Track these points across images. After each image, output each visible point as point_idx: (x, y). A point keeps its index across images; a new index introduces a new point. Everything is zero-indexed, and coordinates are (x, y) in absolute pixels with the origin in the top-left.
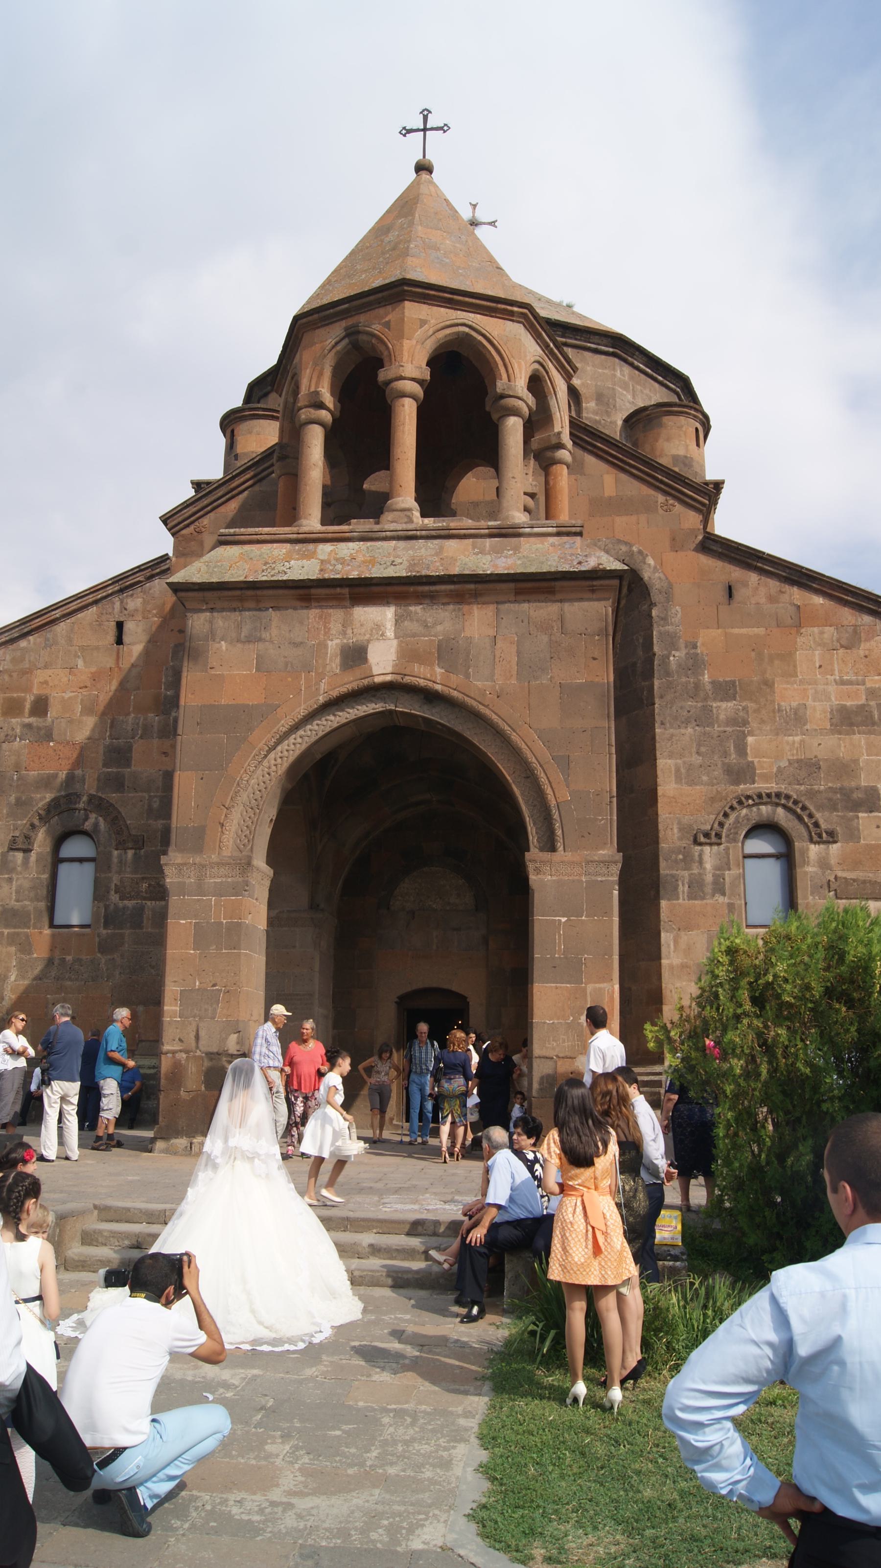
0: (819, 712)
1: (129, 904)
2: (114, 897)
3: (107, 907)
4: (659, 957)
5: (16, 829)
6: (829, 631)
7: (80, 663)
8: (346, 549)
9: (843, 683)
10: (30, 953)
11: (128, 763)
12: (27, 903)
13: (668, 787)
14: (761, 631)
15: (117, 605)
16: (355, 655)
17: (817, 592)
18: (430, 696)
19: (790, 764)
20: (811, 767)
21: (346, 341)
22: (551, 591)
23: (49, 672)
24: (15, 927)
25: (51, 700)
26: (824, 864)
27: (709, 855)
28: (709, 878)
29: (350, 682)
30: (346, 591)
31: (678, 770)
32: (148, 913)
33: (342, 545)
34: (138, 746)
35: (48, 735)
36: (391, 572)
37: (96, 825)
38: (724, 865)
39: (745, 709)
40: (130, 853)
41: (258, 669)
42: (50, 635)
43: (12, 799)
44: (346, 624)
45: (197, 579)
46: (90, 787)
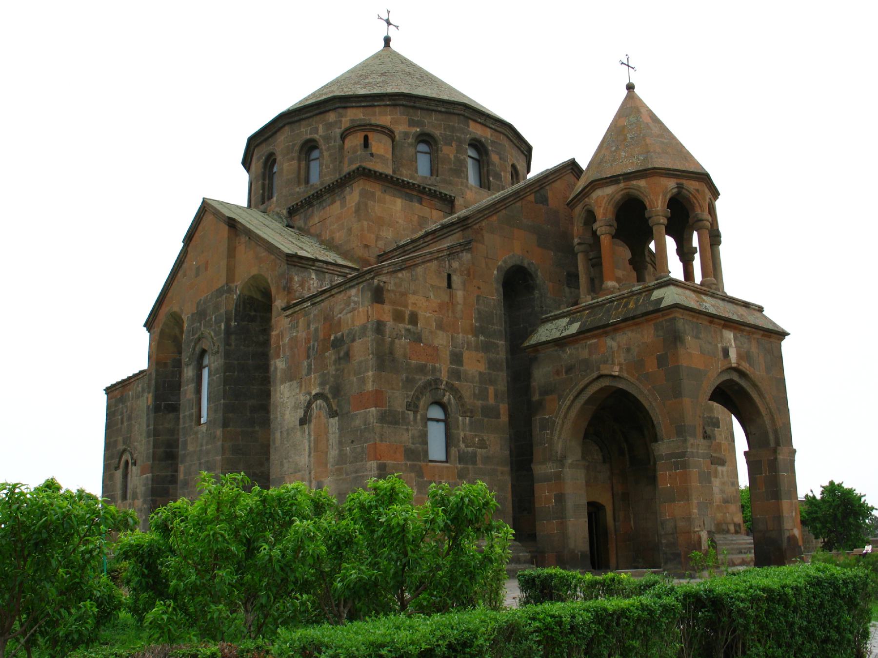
1: (470, 449)
2: (462, 446)
3: (459, 451)
5: (408, 397)
7: (432, 297)
10: (422, 477)
12: (418, 445)
16: (726, 352)
21: (676, 190)
22: (770, 337)
23: (416, 297)
24: (413, 460)
25: (419, 317)
30: (723, 322)
32: (479, 458)
34: (466, 355)
35: (417, 338)
37: (449, 399)
42: (414, 273)
43: (404, 376)
44: (722, 337)
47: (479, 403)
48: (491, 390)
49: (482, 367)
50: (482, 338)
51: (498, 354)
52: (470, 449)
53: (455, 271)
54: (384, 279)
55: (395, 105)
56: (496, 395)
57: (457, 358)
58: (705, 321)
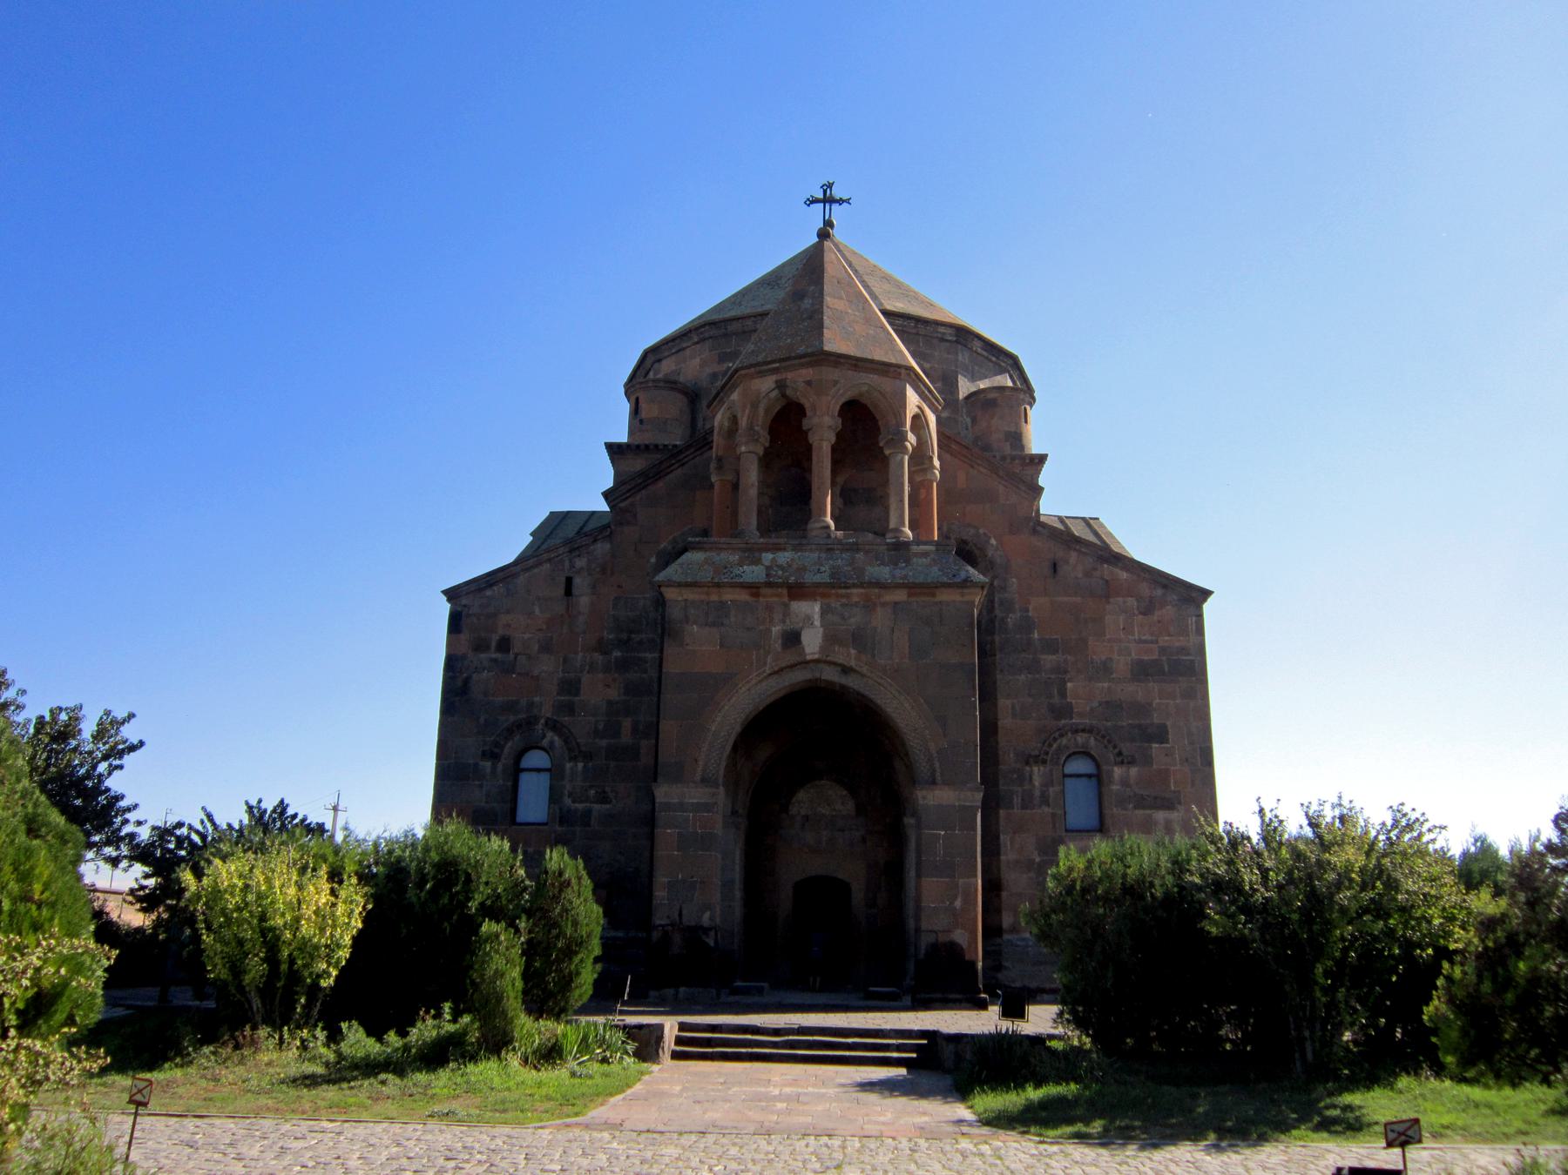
0: (1122, 664)
1: (580, 806)
2: (568, 801)
4: (999, 854)
6: (1132, 602)
8: (784, 557)
9: (1141, 641)
11: (577, 693)
13: (1005, 722)
14: (1079, 599)
15: (567, 564)
16: (792, 639)
17: (1123, 569)
18: (846, 670)
19: (1100, 704)
20: (1112, 707)
26: (1125, 782)
27: (1037, 773)
28: (1037, 793)
29: (790, 658)
31: (1013, 707)
33: (780, 554)
34: (586, 679)
36: (817, 578)
37: (552, 742)
38: (1048, 783)
39: (1065, 661)
40: (580, 765)
41: (722, 646)
43: (482, 720)
44: (786, 613)
45: (676, 578)
46: (547, 712)
47: (604, 743)
48: (627, 723)
49: (614, 694)
50: (617, 654)
51: (645, 671)
52: (580, 806)
53: (579, 572)
54: (464, 602)
55: (703, 340)
56: (635, 730)
57: (570, 687)
58: (744, 596)
